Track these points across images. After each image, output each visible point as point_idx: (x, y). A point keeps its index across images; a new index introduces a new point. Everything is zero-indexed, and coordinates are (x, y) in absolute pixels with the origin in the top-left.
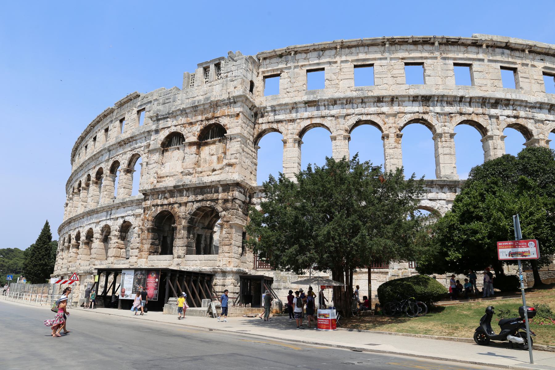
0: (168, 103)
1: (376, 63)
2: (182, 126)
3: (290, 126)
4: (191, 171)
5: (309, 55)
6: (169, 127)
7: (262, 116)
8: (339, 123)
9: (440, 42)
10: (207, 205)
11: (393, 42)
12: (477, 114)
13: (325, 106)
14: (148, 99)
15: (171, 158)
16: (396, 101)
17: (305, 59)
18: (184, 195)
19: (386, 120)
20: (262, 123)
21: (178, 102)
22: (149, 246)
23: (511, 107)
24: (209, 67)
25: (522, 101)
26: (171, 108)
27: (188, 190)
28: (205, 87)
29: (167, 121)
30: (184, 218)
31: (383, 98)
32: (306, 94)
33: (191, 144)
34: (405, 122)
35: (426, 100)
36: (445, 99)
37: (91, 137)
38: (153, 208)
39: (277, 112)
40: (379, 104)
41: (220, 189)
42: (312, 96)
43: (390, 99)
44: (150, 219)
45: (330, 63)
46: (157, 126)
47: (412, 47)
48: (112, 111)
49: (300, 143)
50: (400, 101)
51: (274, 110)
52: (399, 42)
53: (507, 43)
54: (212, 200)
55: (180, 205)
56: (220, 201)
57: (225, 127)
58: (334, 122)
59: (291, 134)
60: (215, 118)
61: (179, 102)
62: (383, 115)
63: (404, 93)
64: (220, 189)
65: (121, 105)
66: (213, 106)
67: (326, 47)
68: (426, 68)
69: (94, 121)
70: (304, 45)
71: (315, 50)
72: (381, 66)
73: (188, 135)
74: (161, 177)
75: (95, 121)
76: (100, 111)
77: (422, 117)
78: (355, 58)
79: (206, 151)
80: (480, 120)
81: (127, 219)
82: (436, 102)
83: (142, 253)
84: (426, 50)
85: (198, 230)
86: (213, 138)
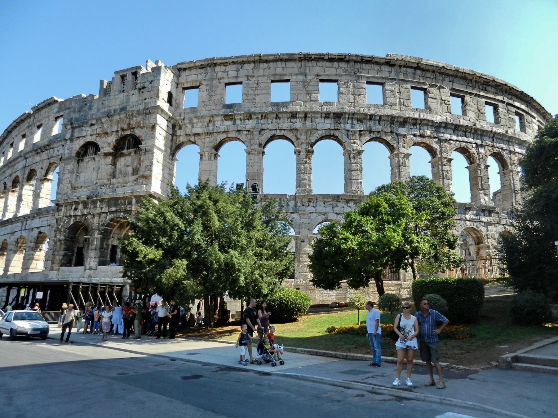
1: (293, 79)
4: (106, 182)
5: (228, 68)
7: (180, 128)
8: (254, 138)
9: (355, 60)
10: (121, 217)
12: (385, 132)
13: (241, 120)
16: (309, 117)
17: (224, 72)
18: (98, 206)
20: (180, 136)
21: (94, 111)
22: (61, 257)
23: (418, 126)
24: (125, 76)
25: (428, 121)
27: (101, 201)
29: (82, 130)
31: (296, 114)
34: (317, 138)
35: (338, 116)
36: (356, 116)
37: (8, 143)
38: (65, 218)
39: (195, 125)
40: (293, 120)
41: (134, 201)
42: (229, 110)
43: (303, 115)
44: (62, 230)
46: (72, 135)
47: (328, 64)
48: (29, 116)
49: (216, 156)
50: (313, 117)
52: (315, 58)
53: (418, 63)
54: (125, 212)
56: (133, 213)
57: (140, 139)
58: (249, 136)
59: (207, 147)
60: (131, 128)
64: (134, 201)
65: (38, 109)
66: (129, 116)
67: (245, 59)
69: (10, 126)
71: (233, 63)
72: (297, 82)
73: (105, 145)
75: (12, 126)
76: (16, 116)
77: (333, 134)
78: (274, 73)
79: (121, 162)
80: (388, 138)
81: (42, 230)
82: (347, 120)
83: (54, 265)
84: (341, 68)
85: (112, 241)
86: (129, 149)
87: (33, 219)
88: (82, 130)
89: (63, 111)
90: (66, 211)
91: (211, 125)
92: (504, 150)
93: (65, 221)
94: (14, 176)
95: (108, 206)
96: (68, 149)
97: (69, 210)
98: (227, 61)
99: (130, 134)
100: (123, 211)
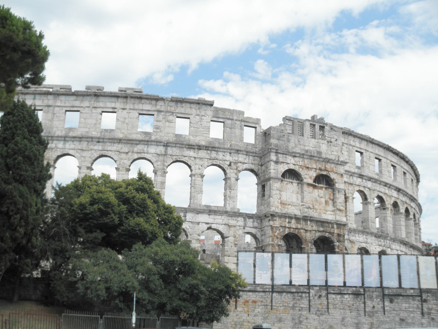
2: (299, 166)
10: (326, 236)
15: (286, 189)
18: (309, 224)
29: (286, 158)
41: (335, 226)
46: (277, 159)
54: (330, 233)
56: (335, 235)
64: (335, 226)
73: (307, 177)
79: (316, 192)
87: (198, 214)
88: (286, 158)
89: (223, 118)
90: (280, 221)
91: (351, 178)
93: (280, 230)
95: (318, 226)
96: (274, 169)
97: (284, 222)
98: (358, 135)
99: (326, 175)
100: (328, 232)
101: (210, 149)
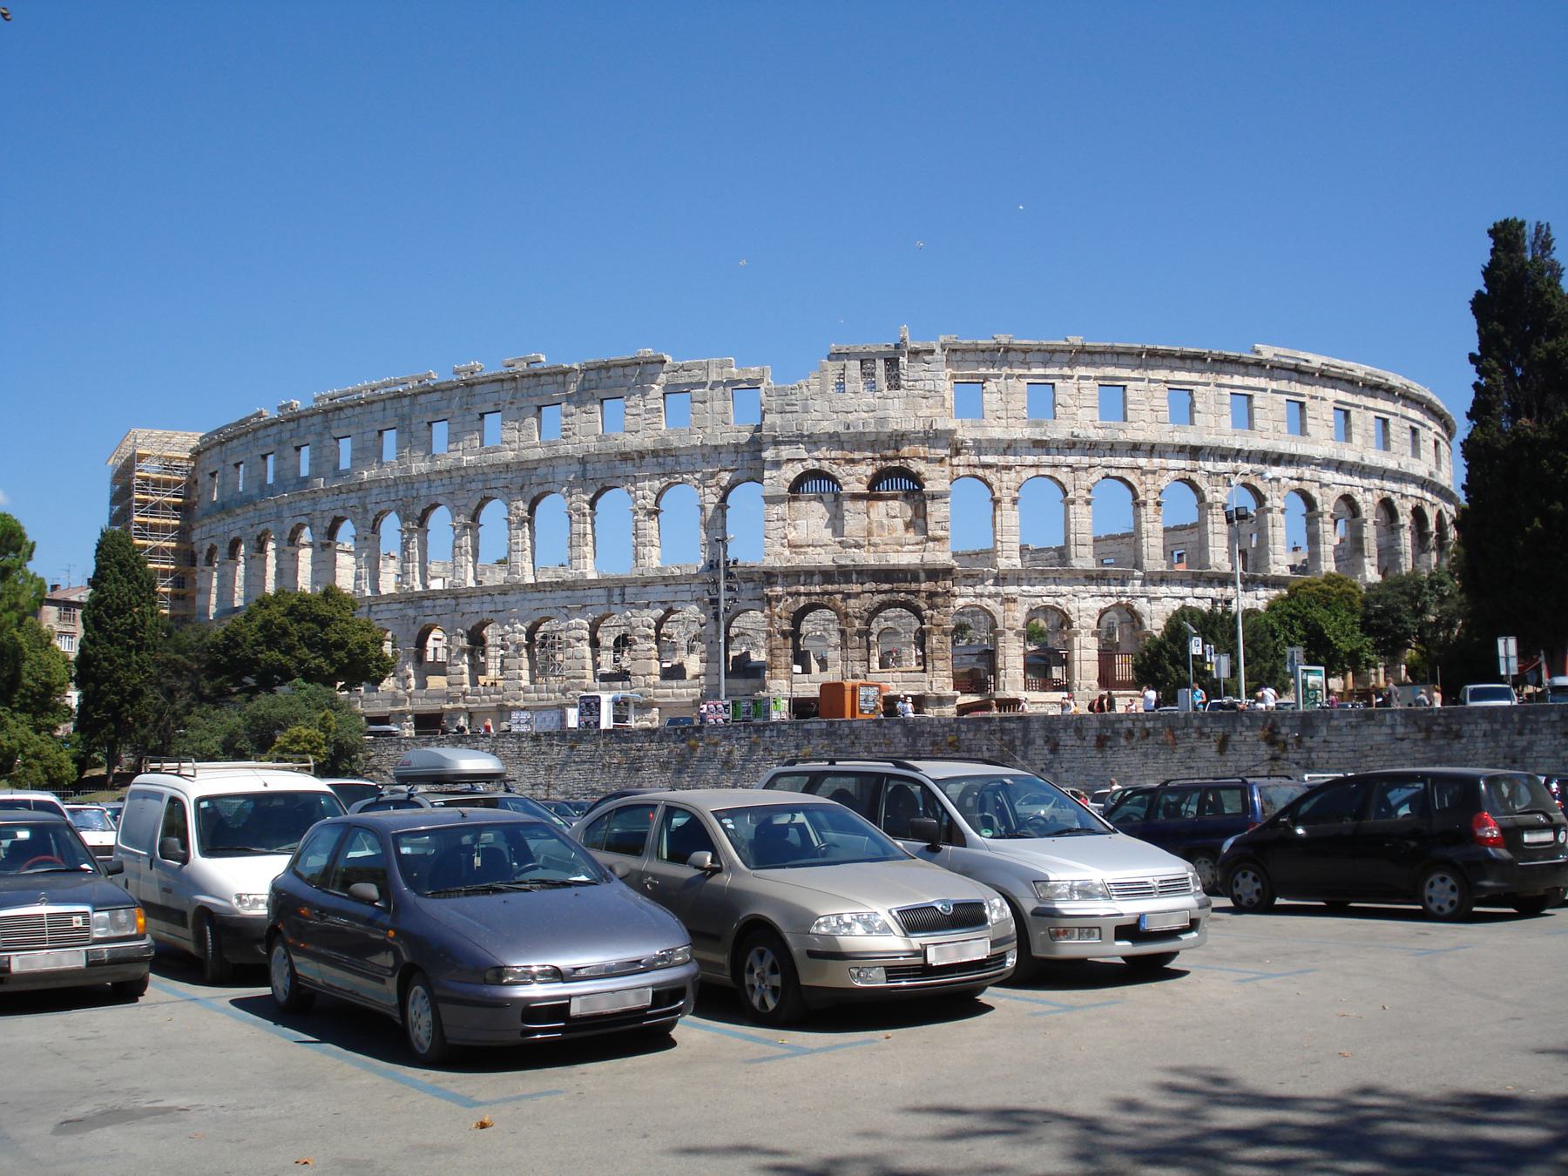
0: (792, 412)
3: (1006, 476)
4: (861, 542)
6: (804, 460)
11: (1152, 354)
13: (1057, 448)
14: (691, 373)
17: (1022, 363)
19: (1143, 478)
20: (959, 466)
26: (802, 425)
28: (869, 399)
30: (857, 618)
32: (1029, 425)
33: (856, 497)
35: (1195, 452)
41: (922, 576)
45: (1063, 377)
47: (1178, 363)
51: (980, 447)
54: (908, 592)
55: (847, 596)
60: (900, 458)
61: (818, 415)
62: (1139, 471)
63: (1166, 439)
64: (922, 576)
68: (1196, 399)
70: (1025, 342)
74: (795, 547)
83: (777, 671)
87: (645, 586)
92: (1394, 492)
94: (535, 492)
101: (661, 454)
